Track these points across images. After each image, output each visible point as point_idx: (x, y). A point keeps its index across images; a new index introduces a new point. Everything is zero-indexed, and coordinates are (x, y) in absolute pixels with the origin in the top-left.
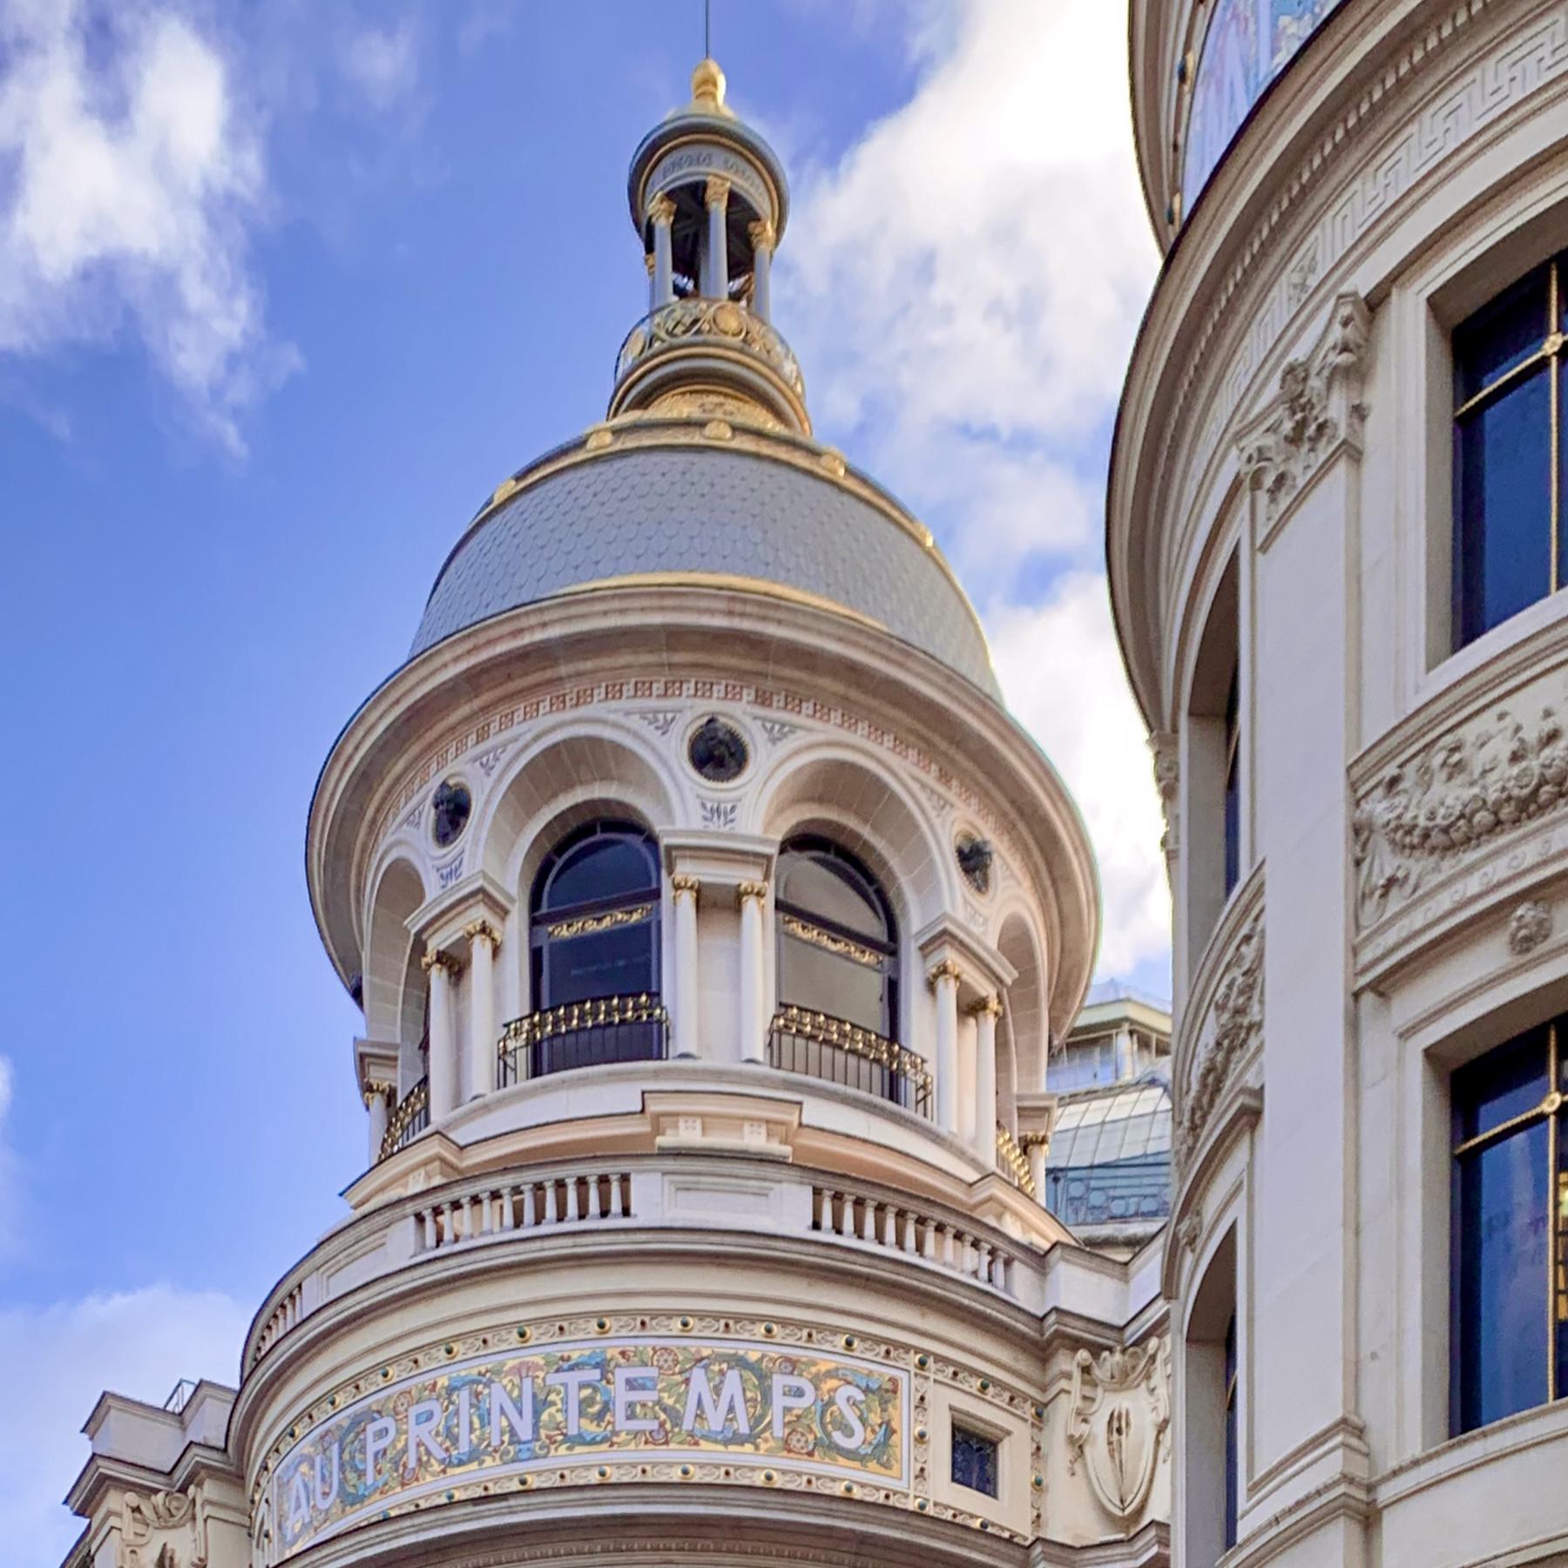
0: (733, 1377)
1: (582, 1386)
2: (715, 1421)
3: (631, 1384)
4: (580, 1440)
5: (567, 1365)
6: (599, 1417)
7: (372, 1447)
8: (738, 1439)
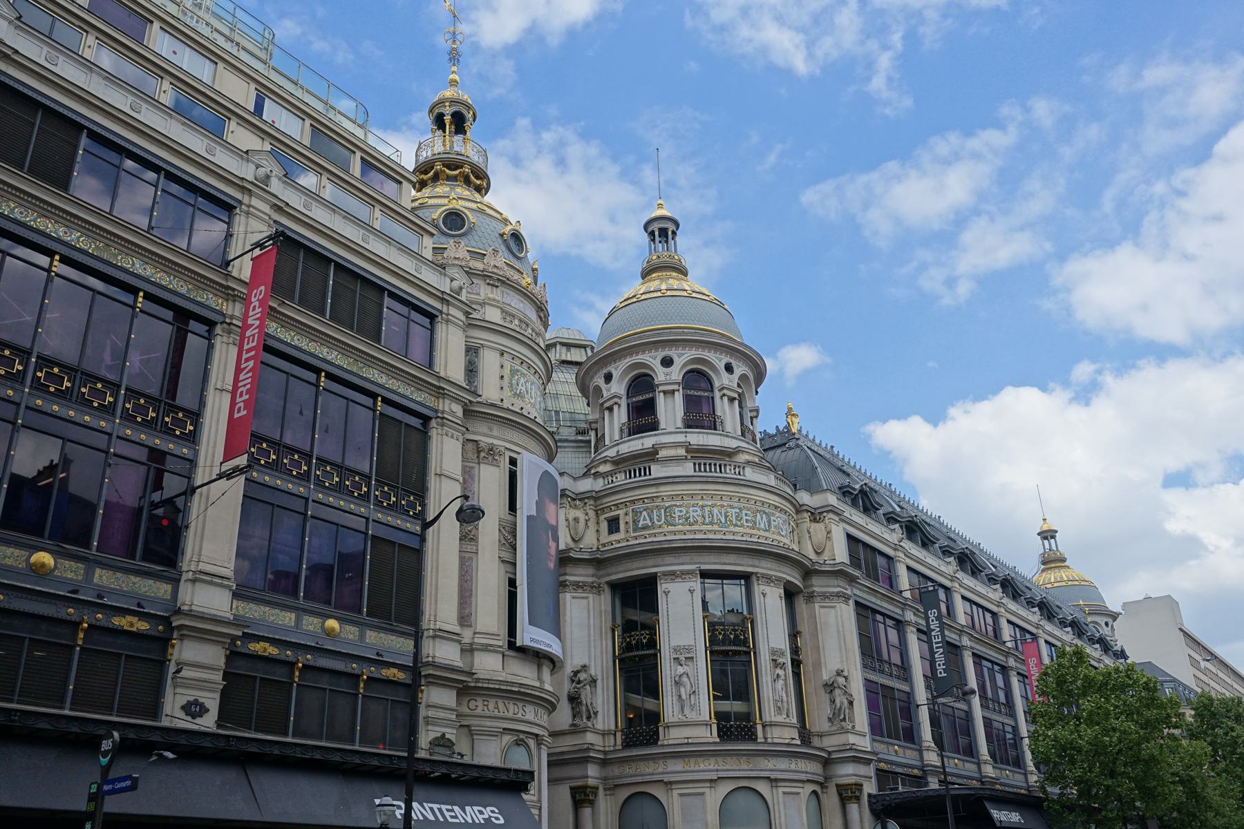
0: (764, 516)
1: (736, 513)
2: (762, 526)
3: (746, 515)
4: (736, 525)
5: (731, 507)
6: (740, 521)
7: (678, 514)
8: (766, 531)
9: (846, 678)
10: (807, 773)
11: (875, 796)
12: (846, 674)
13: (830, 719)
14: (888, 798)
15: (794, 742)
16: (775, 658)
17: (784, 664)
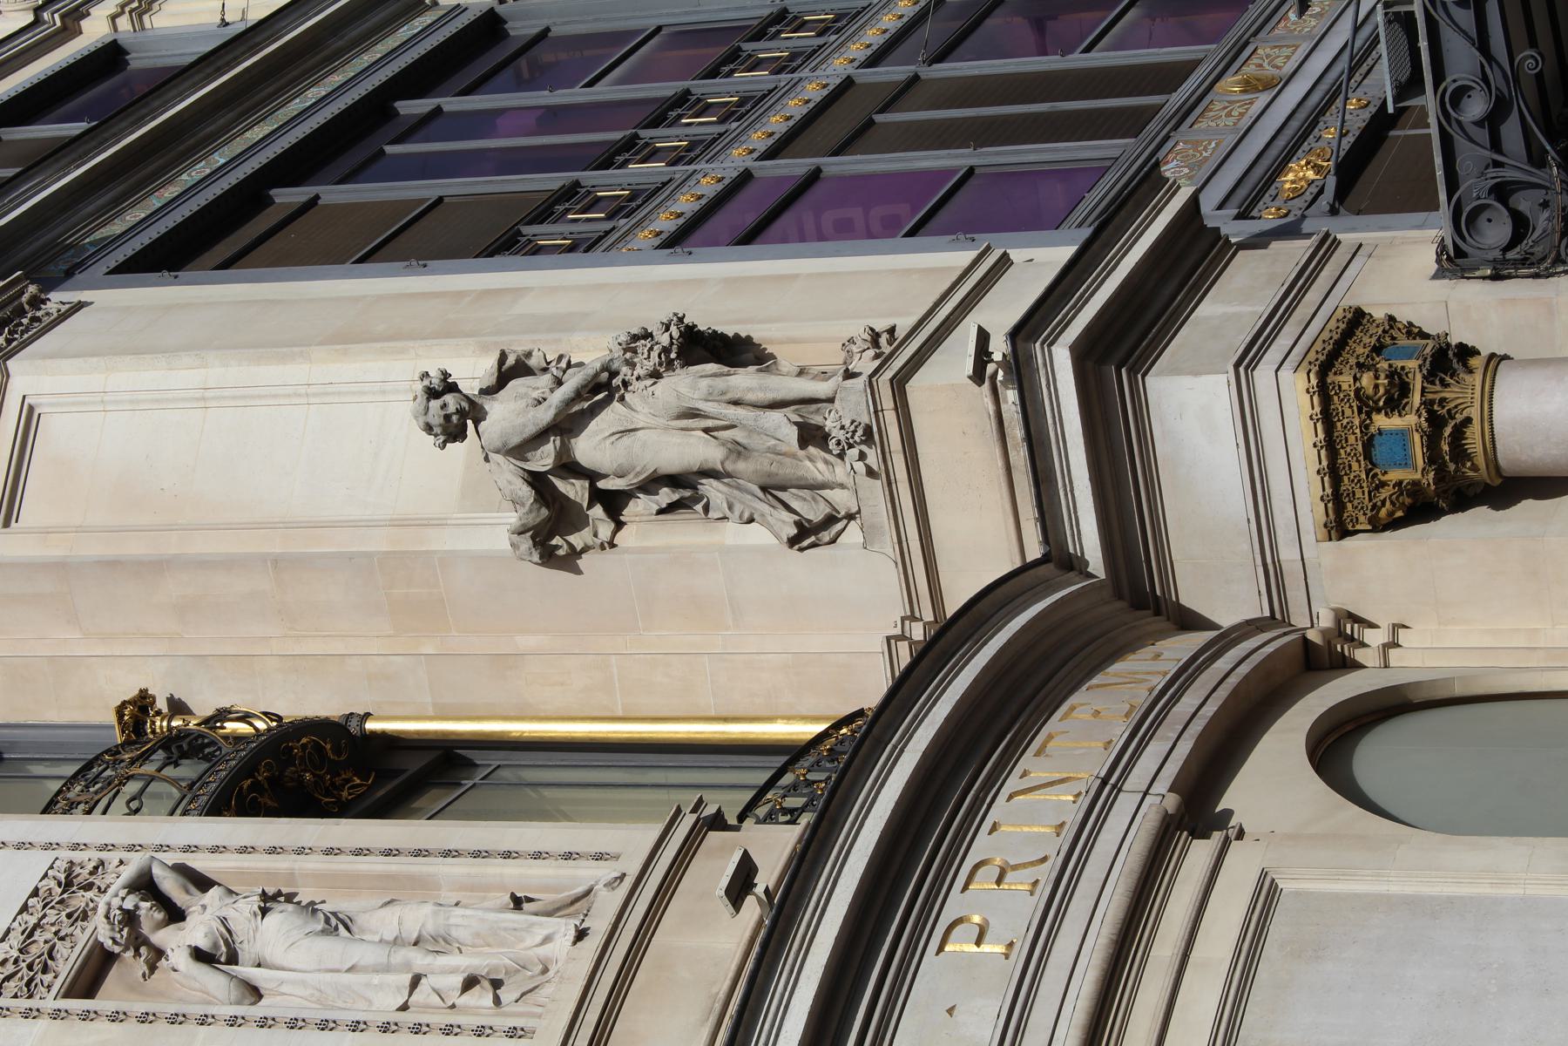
9: (510, 372)
10: (1108, 786)
11: (1464, 221)
12: (473, 372)
13: (805, 535)
14: (1476, 107)
15: (767, 877)
16: (68, 962)
17: (145, 885)
